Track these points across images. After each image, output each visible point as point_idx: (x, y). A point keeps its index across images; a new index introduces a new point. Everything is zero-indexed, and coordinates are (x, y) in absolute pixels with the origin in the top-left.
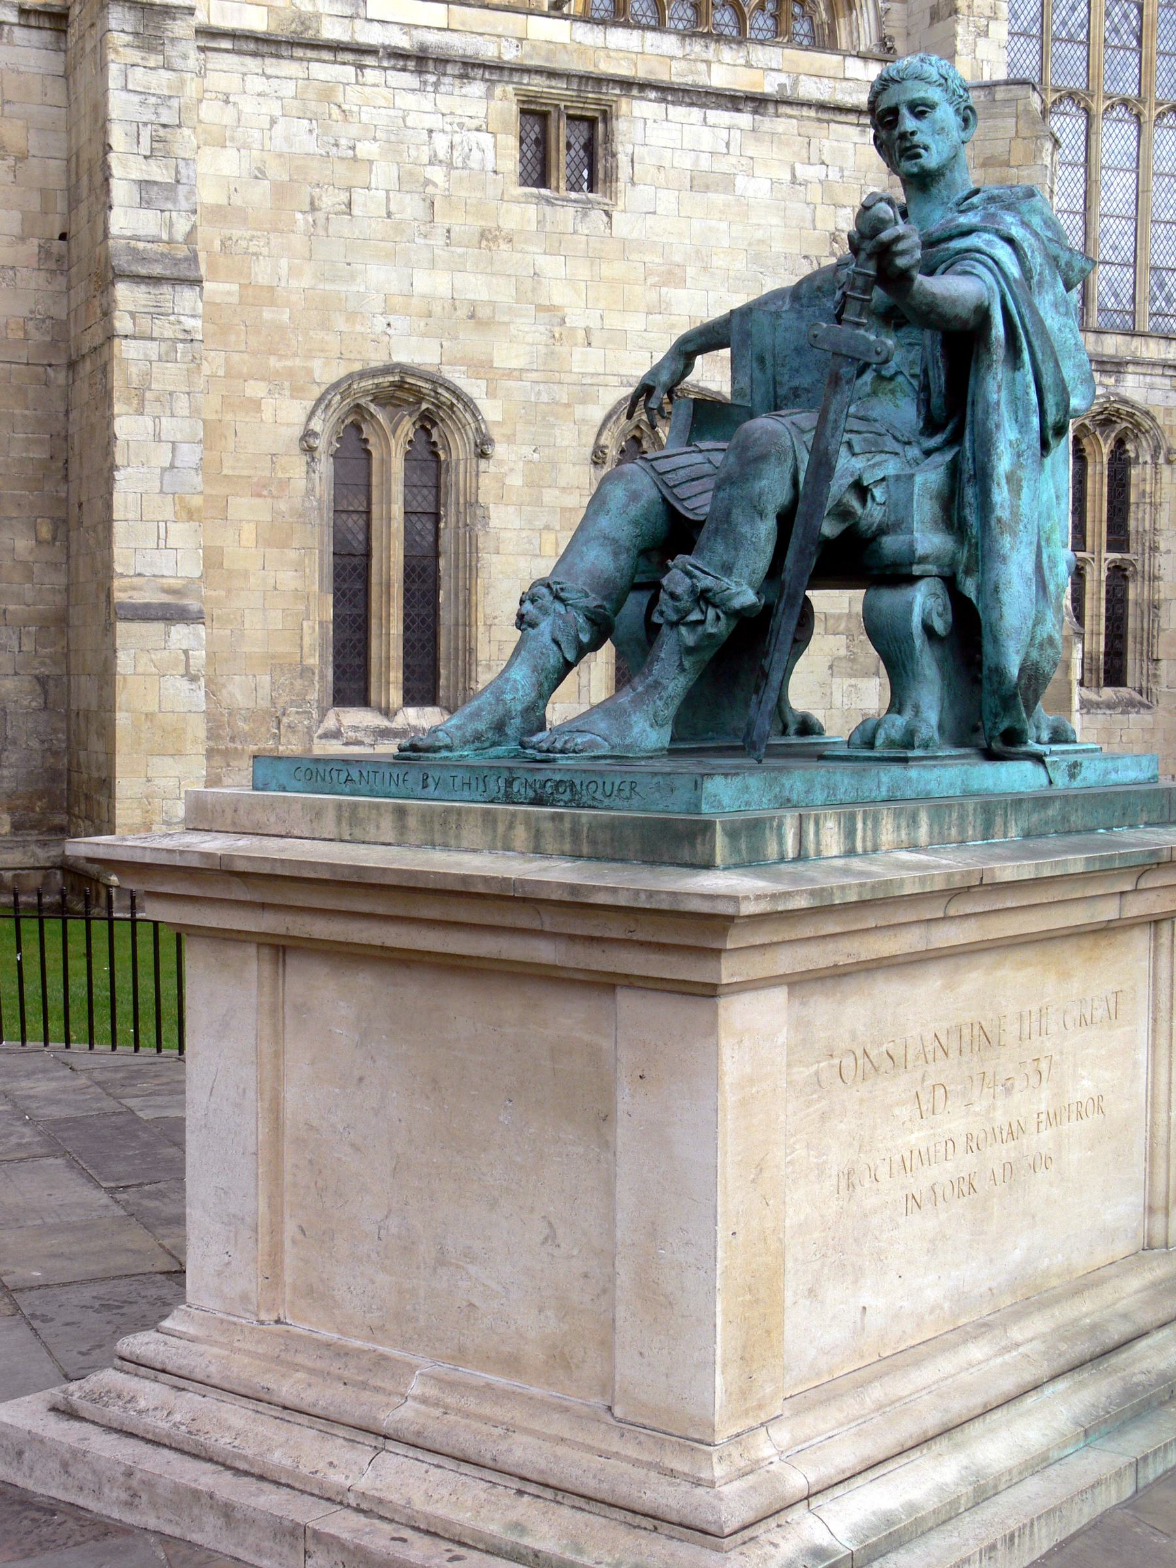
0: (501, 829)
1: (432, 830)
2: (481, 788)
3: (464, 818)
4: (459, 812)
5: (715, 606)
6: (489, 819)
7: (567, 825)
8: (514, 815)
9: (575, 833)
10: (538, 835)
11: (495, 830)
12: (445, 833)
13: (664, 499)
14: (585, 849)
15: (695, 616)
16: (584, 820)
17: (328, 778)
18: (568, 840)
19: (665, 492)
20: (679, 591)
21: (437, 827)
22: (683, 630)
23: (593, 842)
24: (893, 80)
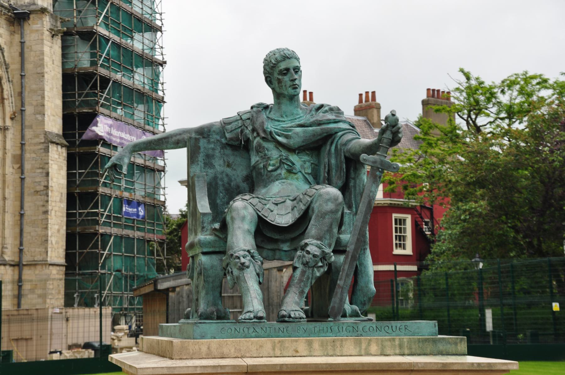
0: (364, 346)
1: (327, 349)
2: (330, 330)
3: (344, 343)
4: (342, 340)
5: (326, 260)
6: (358, 343)
7: (397, 342)
8: (370, 340)
9: (401, 346)
10: (383, 347)
11: (360, 347)
12: (334, 350)
13: (259, 217)
14: (406, 352)
15: (320, 264)
16: (405, 340)
17: (241, 331)
18: (397, 348)
19: (260, 214)
20: (318, 253)
21: (329, 347)
22: (315, 269)
23: (411, 349)
24: (288, 58)
